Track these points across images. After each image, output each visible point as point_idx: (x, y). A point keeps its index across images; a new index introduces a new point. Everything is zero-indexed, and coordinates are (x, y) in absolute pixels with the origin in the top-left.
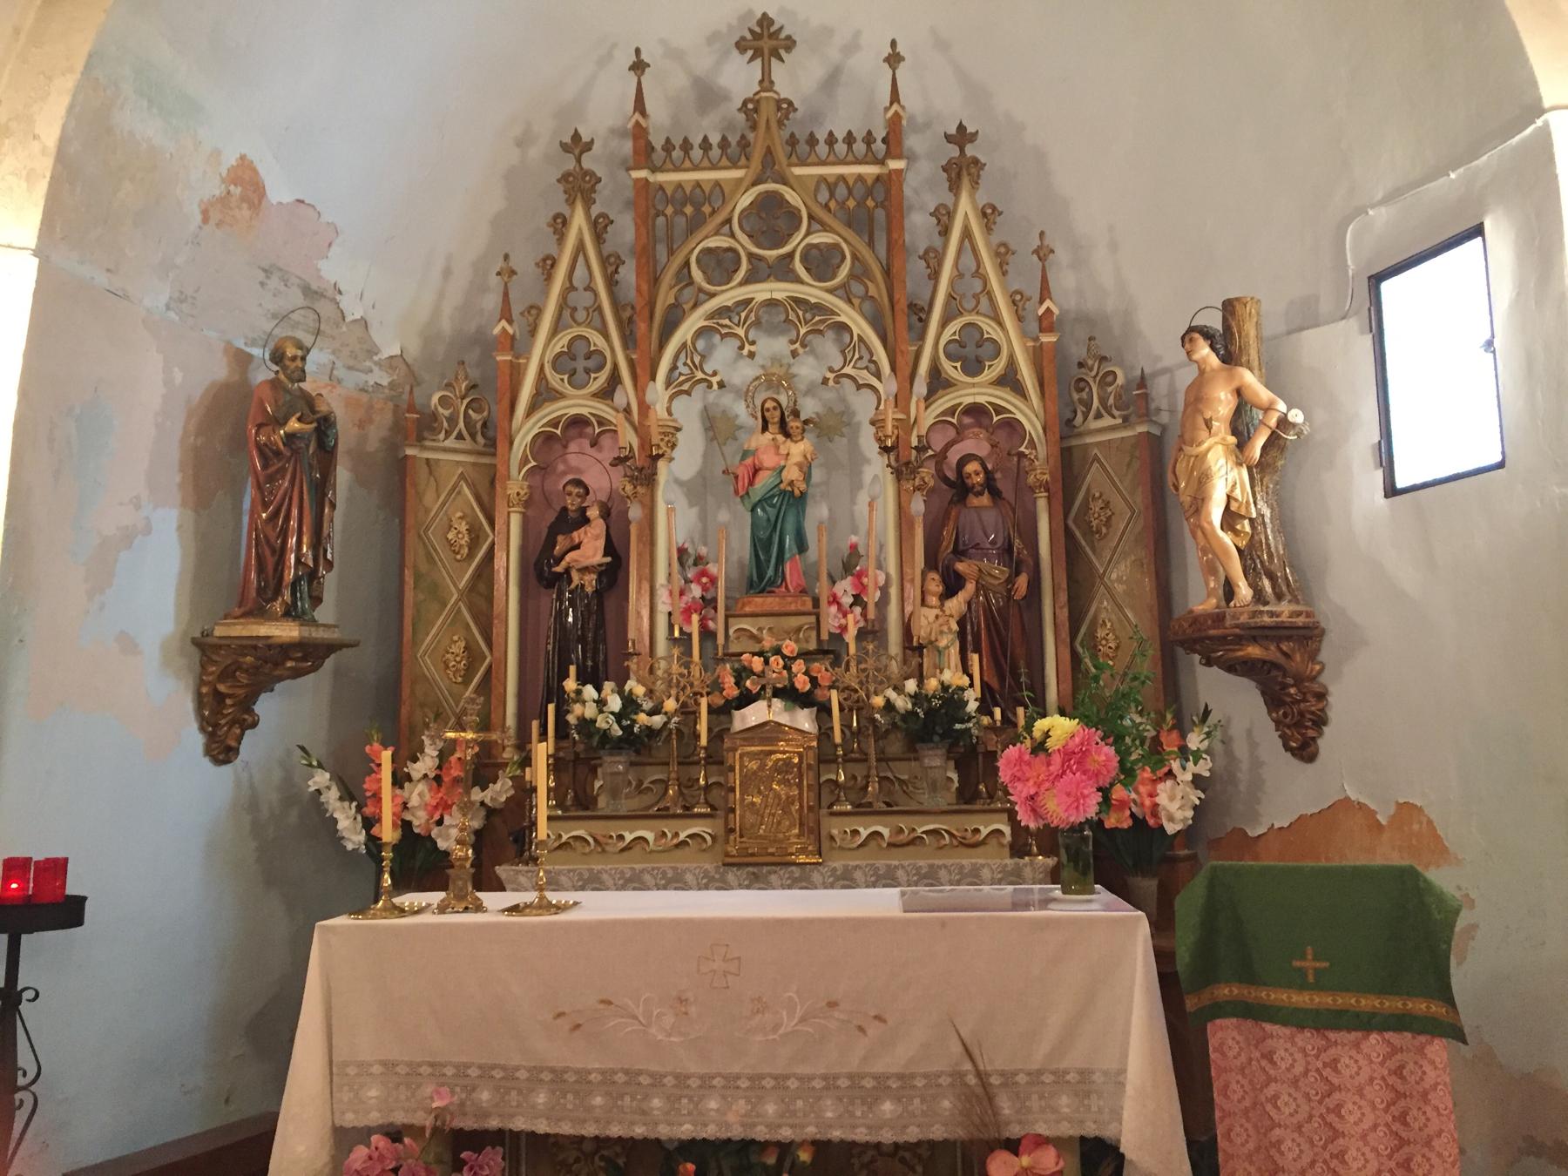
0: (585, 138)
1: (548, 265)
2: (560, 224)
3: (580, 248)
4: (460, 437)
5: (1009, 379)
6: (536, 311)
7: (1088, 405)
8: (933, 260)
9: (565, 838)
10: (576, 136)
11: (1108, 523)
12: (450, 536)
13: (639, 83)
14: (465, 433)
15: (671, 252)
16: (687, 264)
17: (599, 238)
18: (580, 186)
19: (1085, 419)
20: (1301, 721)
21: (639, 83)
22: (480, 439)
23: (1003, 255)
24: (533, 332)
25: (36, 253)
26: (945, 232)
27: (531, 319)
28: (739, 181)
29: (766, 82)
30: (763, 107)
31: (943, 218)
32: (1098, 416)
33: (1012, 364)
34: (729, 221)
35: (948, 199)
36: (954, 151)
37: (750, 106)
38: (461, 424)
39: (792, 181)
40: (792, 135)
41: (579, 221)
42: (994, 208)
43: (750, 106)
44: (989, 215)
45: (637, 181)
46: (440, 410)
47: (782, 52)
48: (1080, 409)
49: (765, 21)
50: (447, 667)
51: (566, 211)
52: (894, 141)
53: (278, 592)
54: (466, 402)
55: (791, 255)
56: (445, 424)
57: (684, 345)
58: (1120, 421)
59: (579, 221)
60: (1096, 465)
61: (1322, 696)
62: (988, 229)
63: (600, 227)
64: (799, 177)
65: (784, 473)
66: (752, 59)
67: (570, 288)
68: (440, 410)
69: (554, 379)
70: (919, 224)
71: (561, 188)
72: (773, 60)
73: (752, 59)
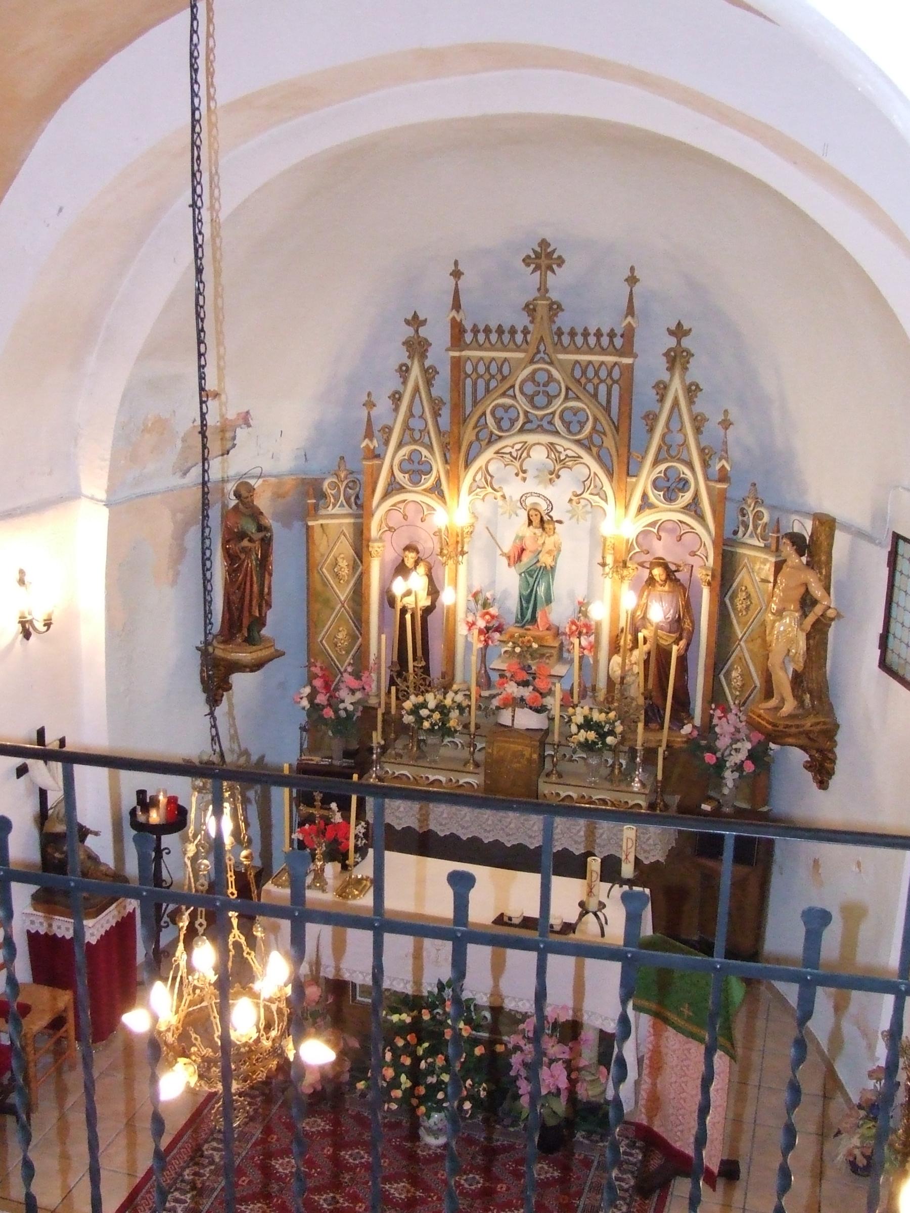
0: (422, 318)
1: (396, 397)
2: (404, 371)
3: (416, 390)
4: (342, 506)
5: (693, 508)
6: (387, 431)
7: (746, 527)
8: (651, 419)
9: (397, 773)
10: (415, 316)
11: (747, 608)
12: (336, 570)
13: (457, 284)
14: (345, 503)
15: (475, 403)
16: (484, 414)
17: (429, 383)
18: (417, 347)
19: (744, 535)
20: (822, 769)
21: (457, 284)
22: (354, 506)
23: (699, 423)
24: (387, 442)
25: (107, 505)
26: (662, 400)
27: (385, 436)
28: (520, 360)
29: (543, 289)
30: (539, 309)
31: (662, 389)
32: (751, 536)
33: (696, 497)
34: (513, 386)
35: (666, 376)
36: (672, 342)
37: (531, 307)
38: (342, 498)
39: (556, 362)
40: (559, 329)
41: (416, 372)
42: (697, 386)
43: (531, 307)
44: (692, 391)
45: (453, 358)
46: (329, 491)
47: (555, 267)
48: (741, 529)
49: (544, 243)
50: (336, 646)
51: (409, 363)
52: (626, 341)
53: (240, 630)
54: (345, 483)
55: (553, 413)
56: (332, 500)
57: (480, 468)
58: (763, 545)
59: (416, 372)
60: (745, 569)
61: (833, 761)
62: (691, 402)
63: (429, 375)
64: (559, 360)
65: (540, 556)
66: (534, 271)
67: (410, 414)
68: (329, 491)
69: (401, 477)
70: (644, 395)
71: (404, 348)
72: (549, 273)
73: (534, 271)
